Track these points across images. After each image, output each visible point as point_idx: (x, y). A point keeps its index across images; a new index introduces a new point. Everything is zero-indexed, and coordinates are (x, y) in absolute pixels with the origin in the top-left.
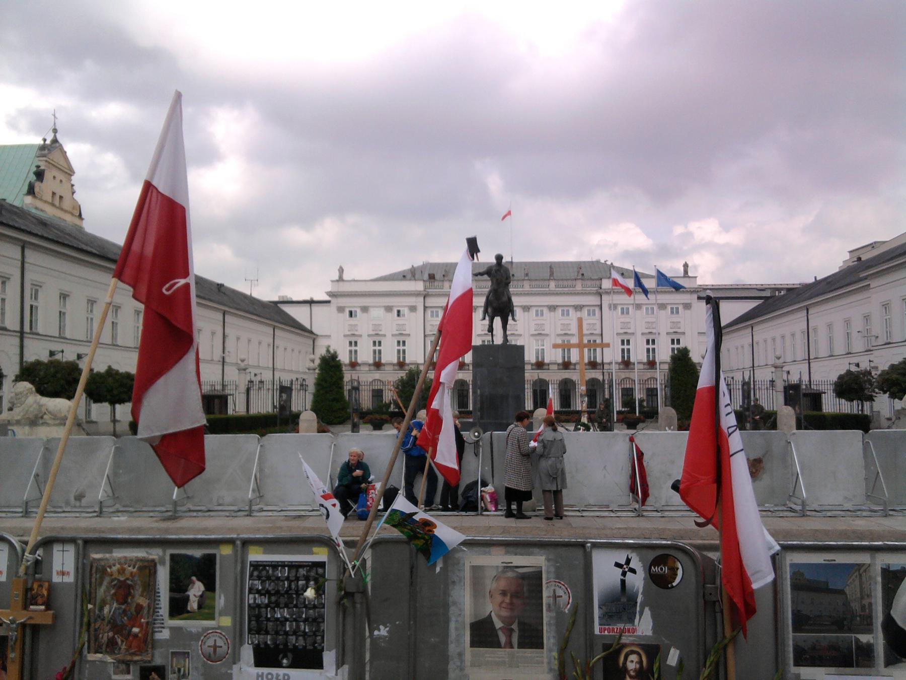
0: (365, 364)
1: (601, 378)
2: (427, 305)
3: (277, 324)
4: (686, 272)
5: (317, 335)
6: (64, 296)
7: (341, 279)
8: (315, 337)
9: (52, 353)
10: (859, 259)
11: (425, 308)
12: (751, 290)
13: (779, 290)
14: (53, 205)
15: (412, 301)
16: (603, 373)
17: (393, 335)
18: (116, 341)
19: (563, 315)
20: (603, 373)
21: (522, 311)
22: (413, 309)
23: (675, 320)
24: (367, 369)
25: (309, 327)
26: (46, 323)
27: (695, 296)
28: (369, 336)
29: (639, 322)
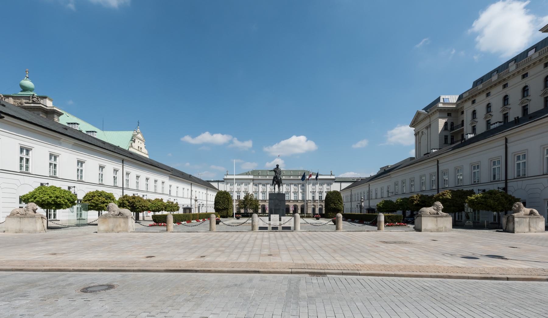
2: (254, 182)
3: (208, 187)
6: (147, 179)
9: (134, 194)
10: (385, 170)
11: (253, 183)
13: (359, 179)
14: (138, 150)
17: (243, 191)
18: (163, 192)
22: (249, 183)
23: (328, 188)
25: (218, 188)
26: (133, 185)
28: (236, 192)
29: (318, 187)
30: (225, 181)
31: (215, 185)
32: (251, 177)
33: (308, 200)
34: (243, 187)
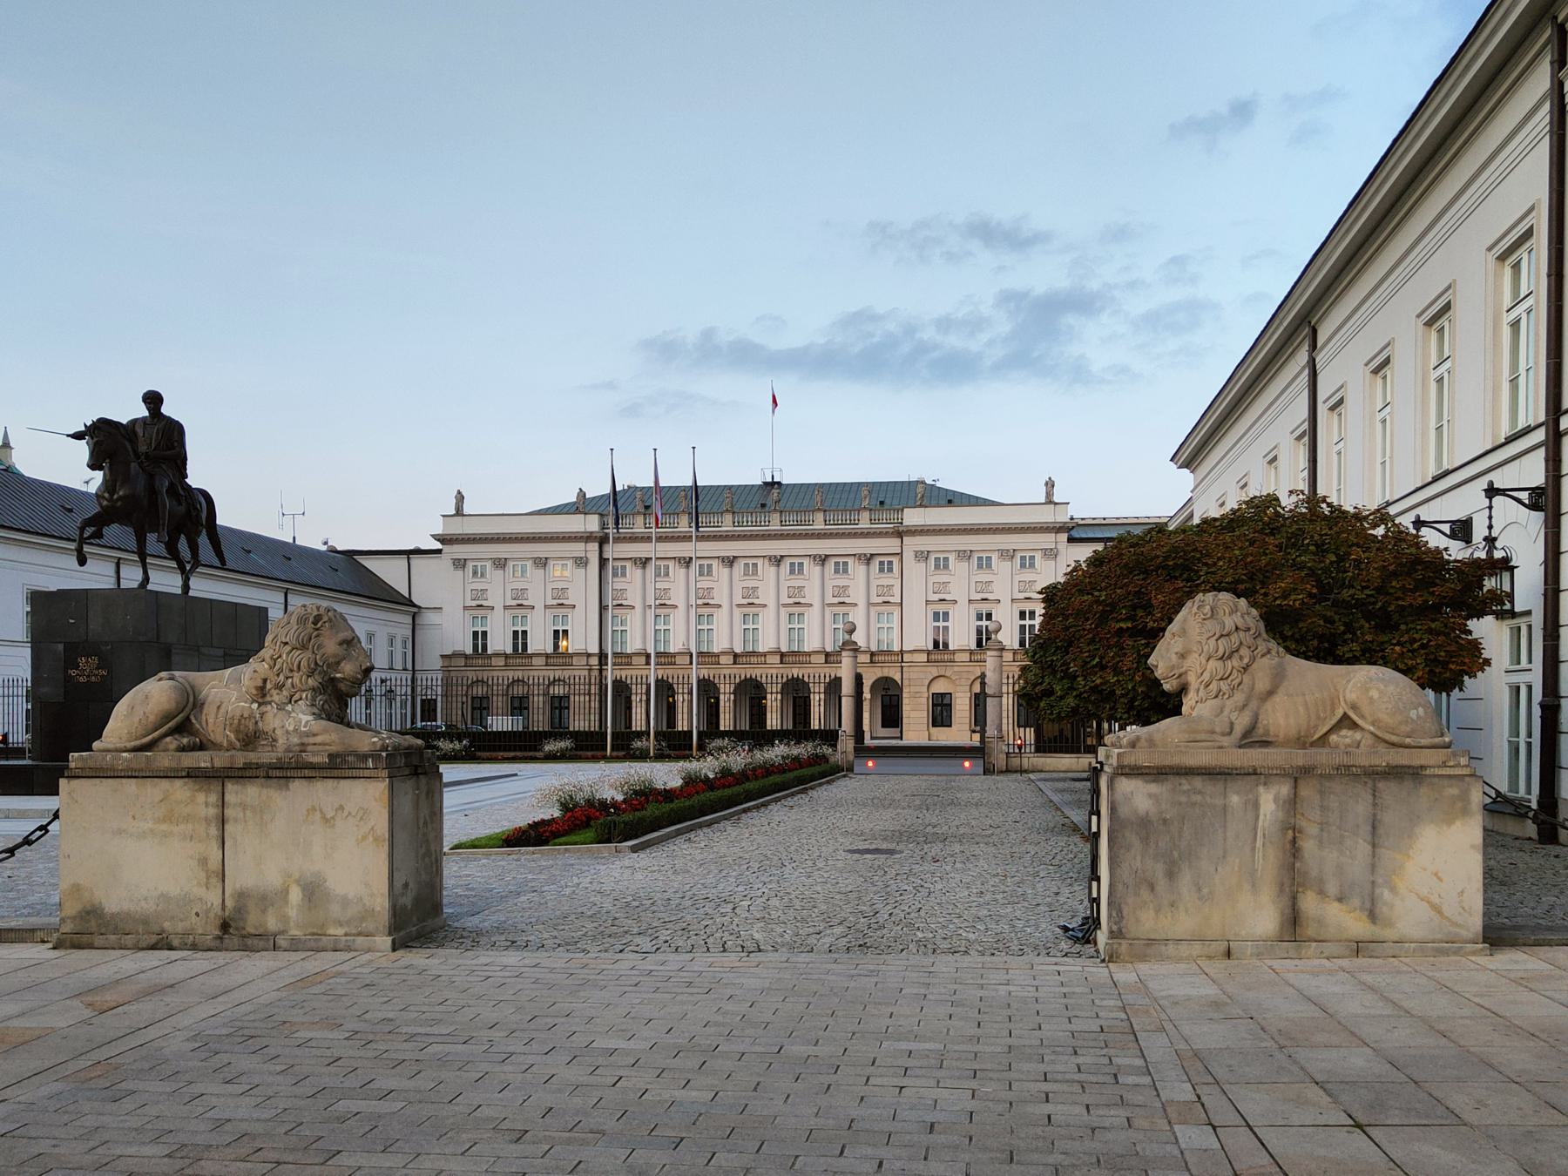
0: (497, 655)
1: (897, 678)
4: (1049, 494)
5: (419, 607)
7: (459, 512)
8: (415, 610)
11: (603, 562)
12: (1102, 527)
15: (577, 549)
16: (902, 667)
19: (837, 571)
20: (902, 667)
21: (766, 561)
22: (582, 562)
24: (503, 664)
27: (1064, 537)
29: (960, 582)
30: (446, 549)
31: (391, 573)
32: (592, 524)
33: (910, 652)
34: (537, 588)
